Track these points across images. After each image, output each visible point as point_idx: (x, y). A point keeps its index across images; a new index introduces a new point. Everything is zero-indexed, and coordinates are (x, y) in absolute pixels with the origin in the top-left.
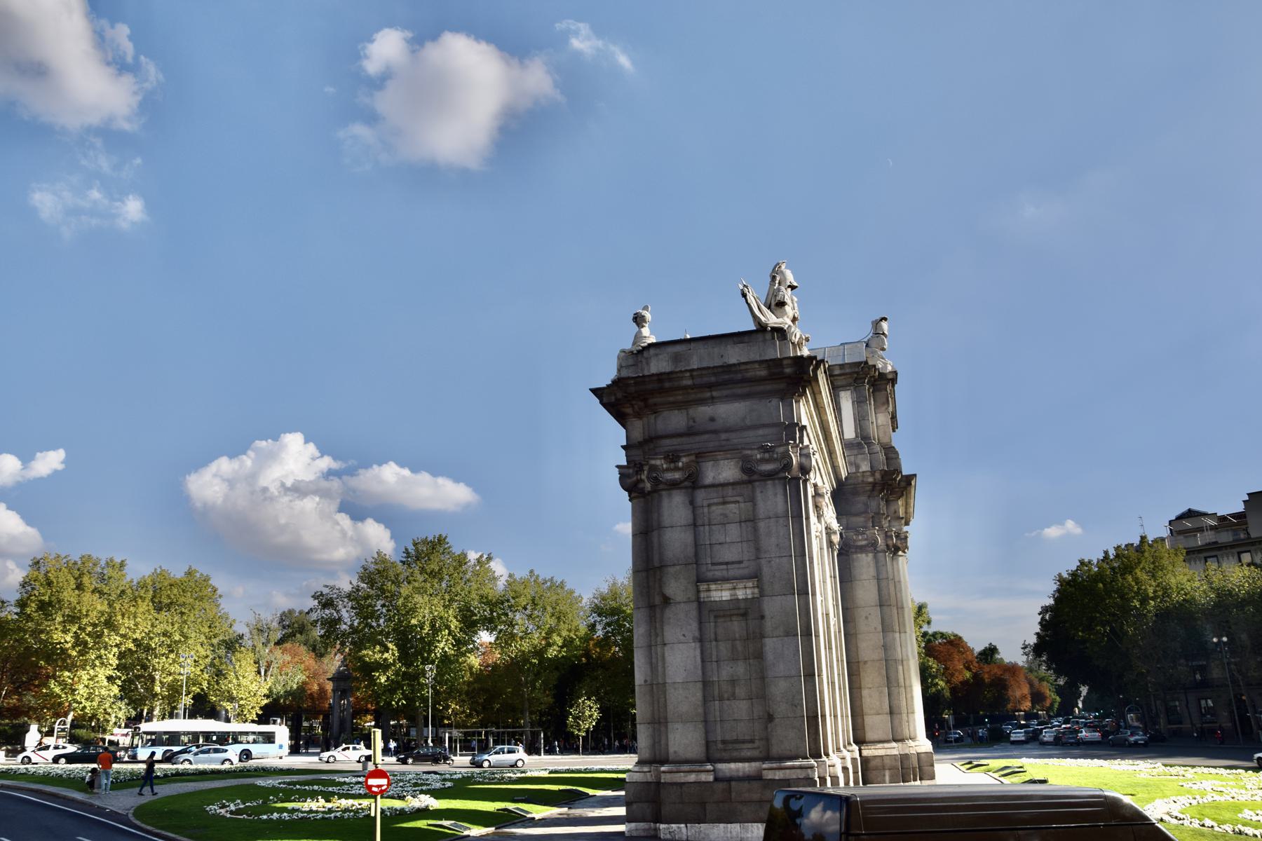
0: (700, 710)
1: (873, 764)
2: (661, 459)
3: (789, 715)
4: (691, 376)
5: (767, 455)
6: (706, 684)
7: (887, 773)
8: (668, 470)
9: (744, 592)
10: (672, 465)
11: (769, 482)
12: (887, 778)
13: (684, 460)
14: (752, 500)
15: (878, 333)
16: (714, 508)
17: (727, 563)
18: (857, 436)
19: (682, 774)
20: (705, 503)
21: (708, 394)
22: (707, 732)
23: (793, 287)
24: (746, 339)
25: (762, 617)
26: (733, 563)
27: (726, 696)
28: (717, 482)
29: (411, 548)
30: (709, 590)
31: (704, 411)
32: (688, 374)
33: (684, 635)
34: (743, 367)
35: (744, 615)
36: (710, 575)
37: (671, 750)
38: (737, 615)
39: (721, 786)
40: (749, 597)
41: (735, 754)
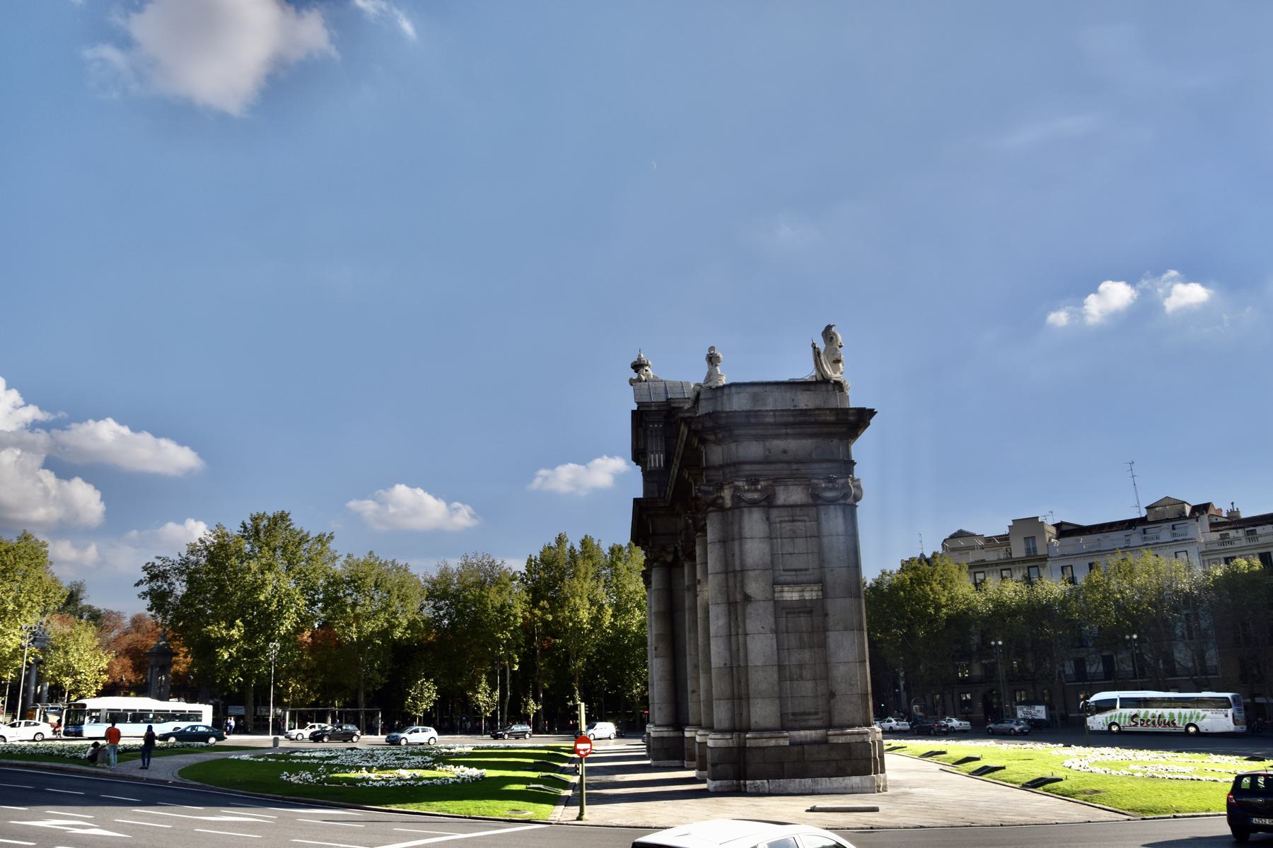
0: (776, 689)
2: (743, 481)
3: (848, 693)
4: (774, 415)
5: (830, 485)
6: (781, 667)
8: (748, 491)
9: (811, 594)
10: (753, 487)
11: (832, 507)
13: (763, 483)
14: (818, 520)
16: (784, 525)
17: (795, 570)
19: (764, 740)
20: (778, 520)
22: (781, 706)
24: (812, 387)
25: (826, 615)
26: (800, 570)
27: (795, 677)
28: (787, 503)
29: (248, 522)
30: (782, 591)
32: (772, 413)
33: (763, 628)
34: (817, 412)
36: (782, 579)
37: (753, 721)
38: (804, 612)
39: (796, 749)
40: (814, 598)
41: (803, 724)
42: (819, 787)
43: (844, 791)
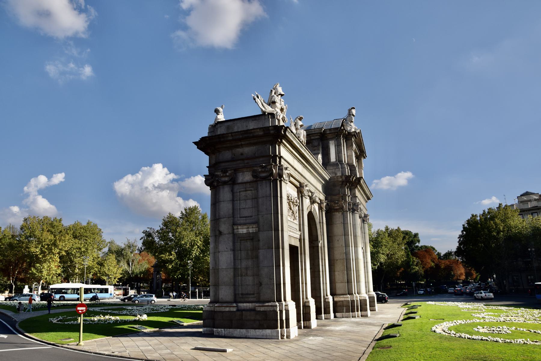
0: (232, 281)
1: (339, 304)
2: (220, 172)
3: (268, 283)
4: (232, 135)
5: (263, 170)
6: (235, 269)
7: (345, 308)
8: (223, 177)
10: (224, 175)
12: (345, 310)
13: (229, 172)
14: (257, 189)
15: (350, 114)
16: (242, 193)
17: (246, 217)
18: (336, 160)
19: (223, 308)
20: (238, 191)
21: (240, 143)
23: (282, 95)
24: (257, 118)
25: (259, 240)
26: (248, 217)
27: (244, 274)
28: (243, 182)
29: (184, 212)
30: (238, 229)
31: (240, 150)
32: (230, 135)
33: (227, 248)
34: (253, 131)
35: (252, 239)
36: (239, 222)
37: (220, 297)
39: (239, 313)
40: (254, 232)
41: (246, 299)
42: (249, 334)
43: (262, 337)
